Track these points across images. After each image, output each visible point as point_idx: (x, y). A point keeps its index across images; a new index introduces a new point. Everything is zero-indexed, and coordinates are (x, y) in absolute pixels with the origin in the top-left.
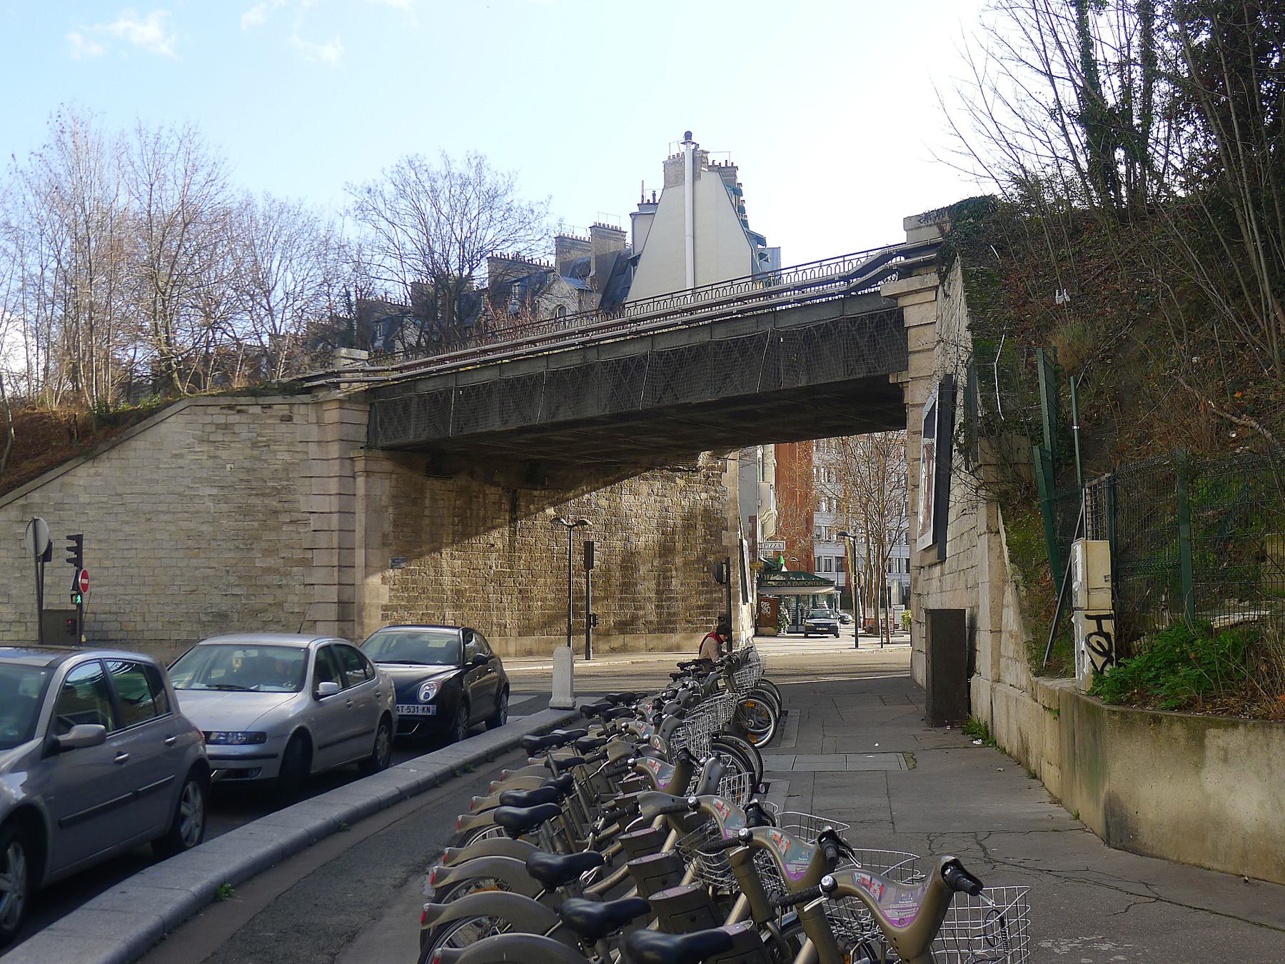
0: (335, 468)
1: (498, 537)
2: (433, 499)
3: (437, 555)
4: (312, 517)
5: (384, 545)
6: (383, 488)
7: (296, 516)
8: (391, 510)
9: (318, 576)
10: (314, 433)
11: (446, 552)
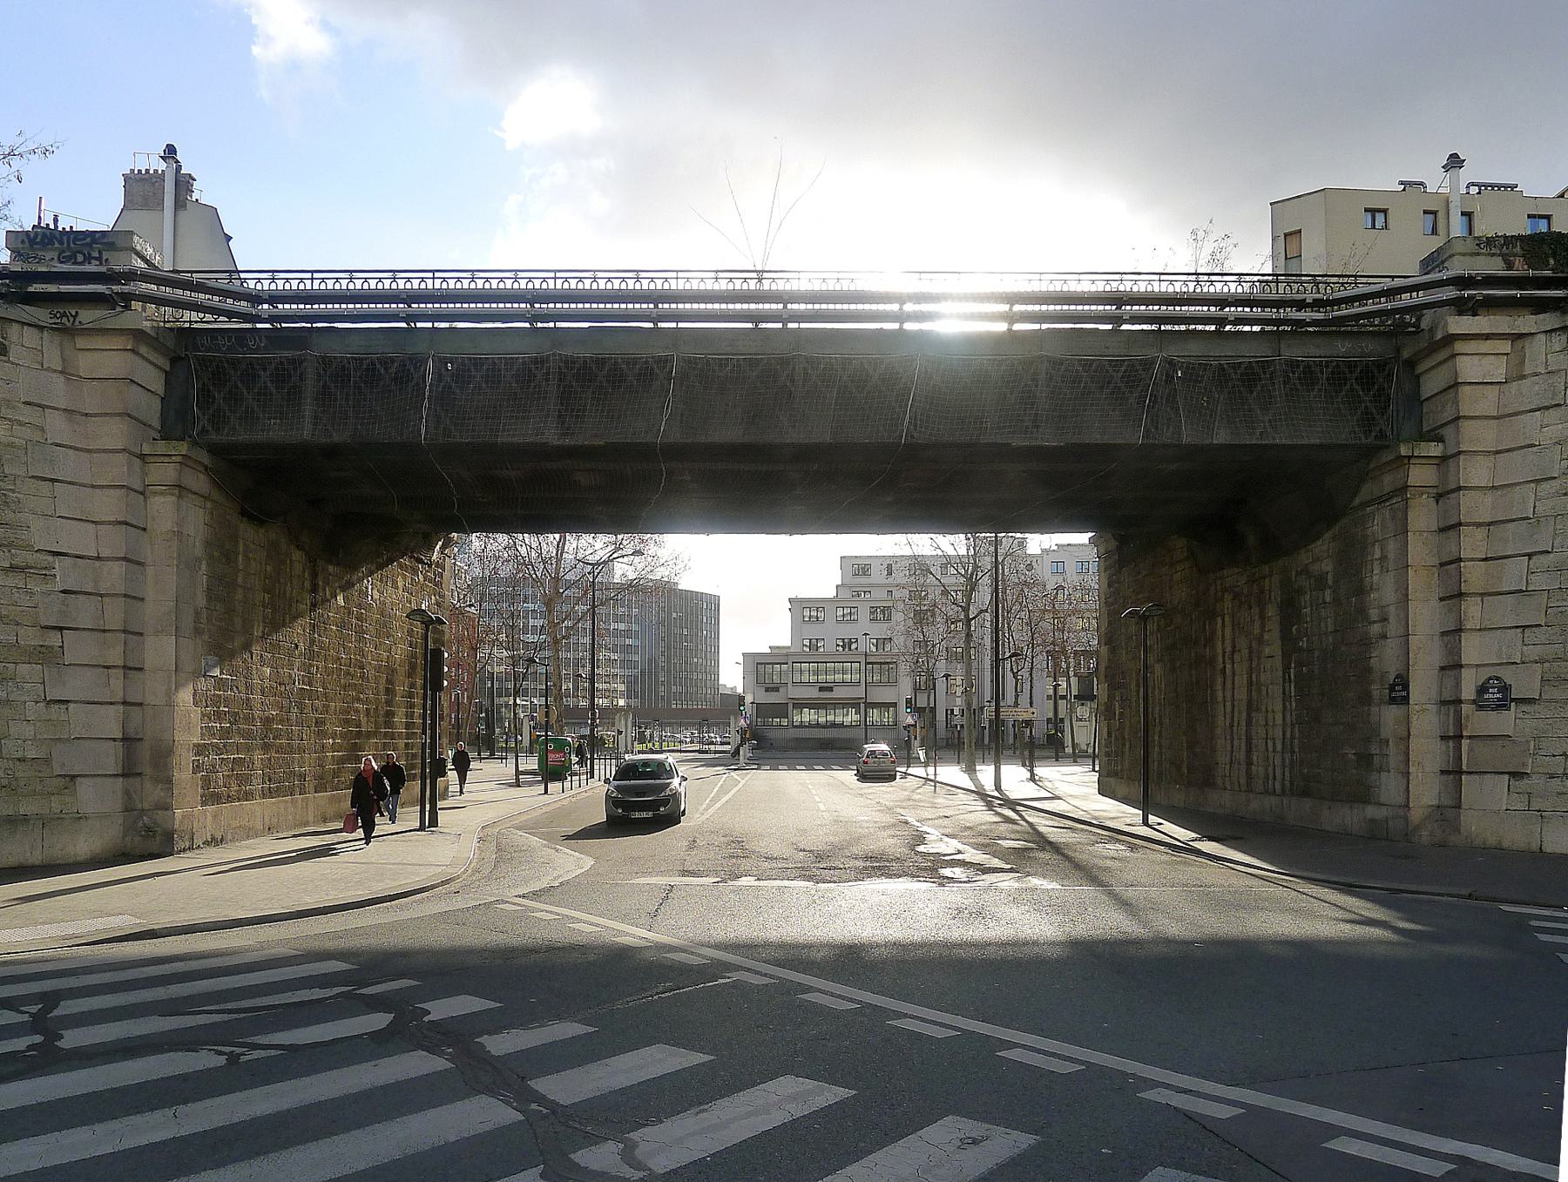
0: (118, 469)
1: (298, 632)
2: (247, 558)
3: (246, 656)
4: (57, 562)
5: (197, 631)
6: (196, 521)
7: (22, 557)
8: (204, 567)
9: (76, 685)
10: (58, 391)
11: (256, 649)
